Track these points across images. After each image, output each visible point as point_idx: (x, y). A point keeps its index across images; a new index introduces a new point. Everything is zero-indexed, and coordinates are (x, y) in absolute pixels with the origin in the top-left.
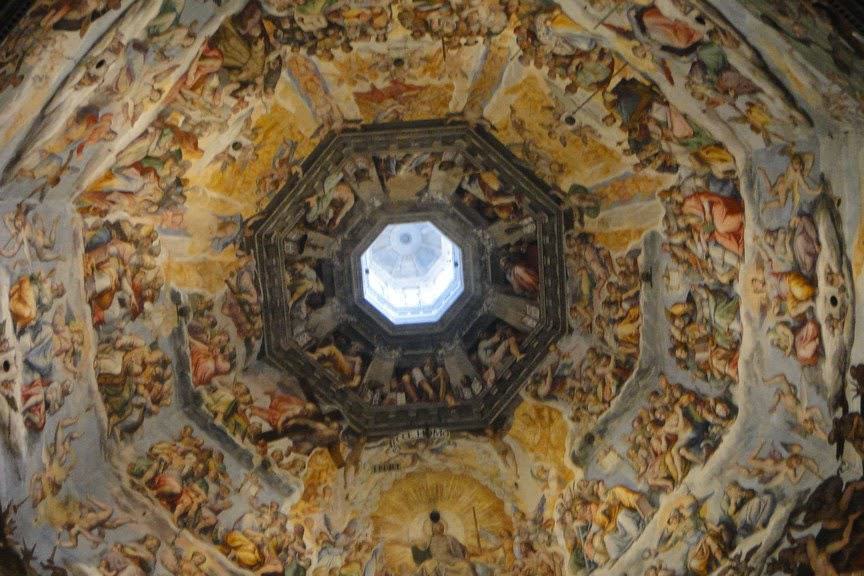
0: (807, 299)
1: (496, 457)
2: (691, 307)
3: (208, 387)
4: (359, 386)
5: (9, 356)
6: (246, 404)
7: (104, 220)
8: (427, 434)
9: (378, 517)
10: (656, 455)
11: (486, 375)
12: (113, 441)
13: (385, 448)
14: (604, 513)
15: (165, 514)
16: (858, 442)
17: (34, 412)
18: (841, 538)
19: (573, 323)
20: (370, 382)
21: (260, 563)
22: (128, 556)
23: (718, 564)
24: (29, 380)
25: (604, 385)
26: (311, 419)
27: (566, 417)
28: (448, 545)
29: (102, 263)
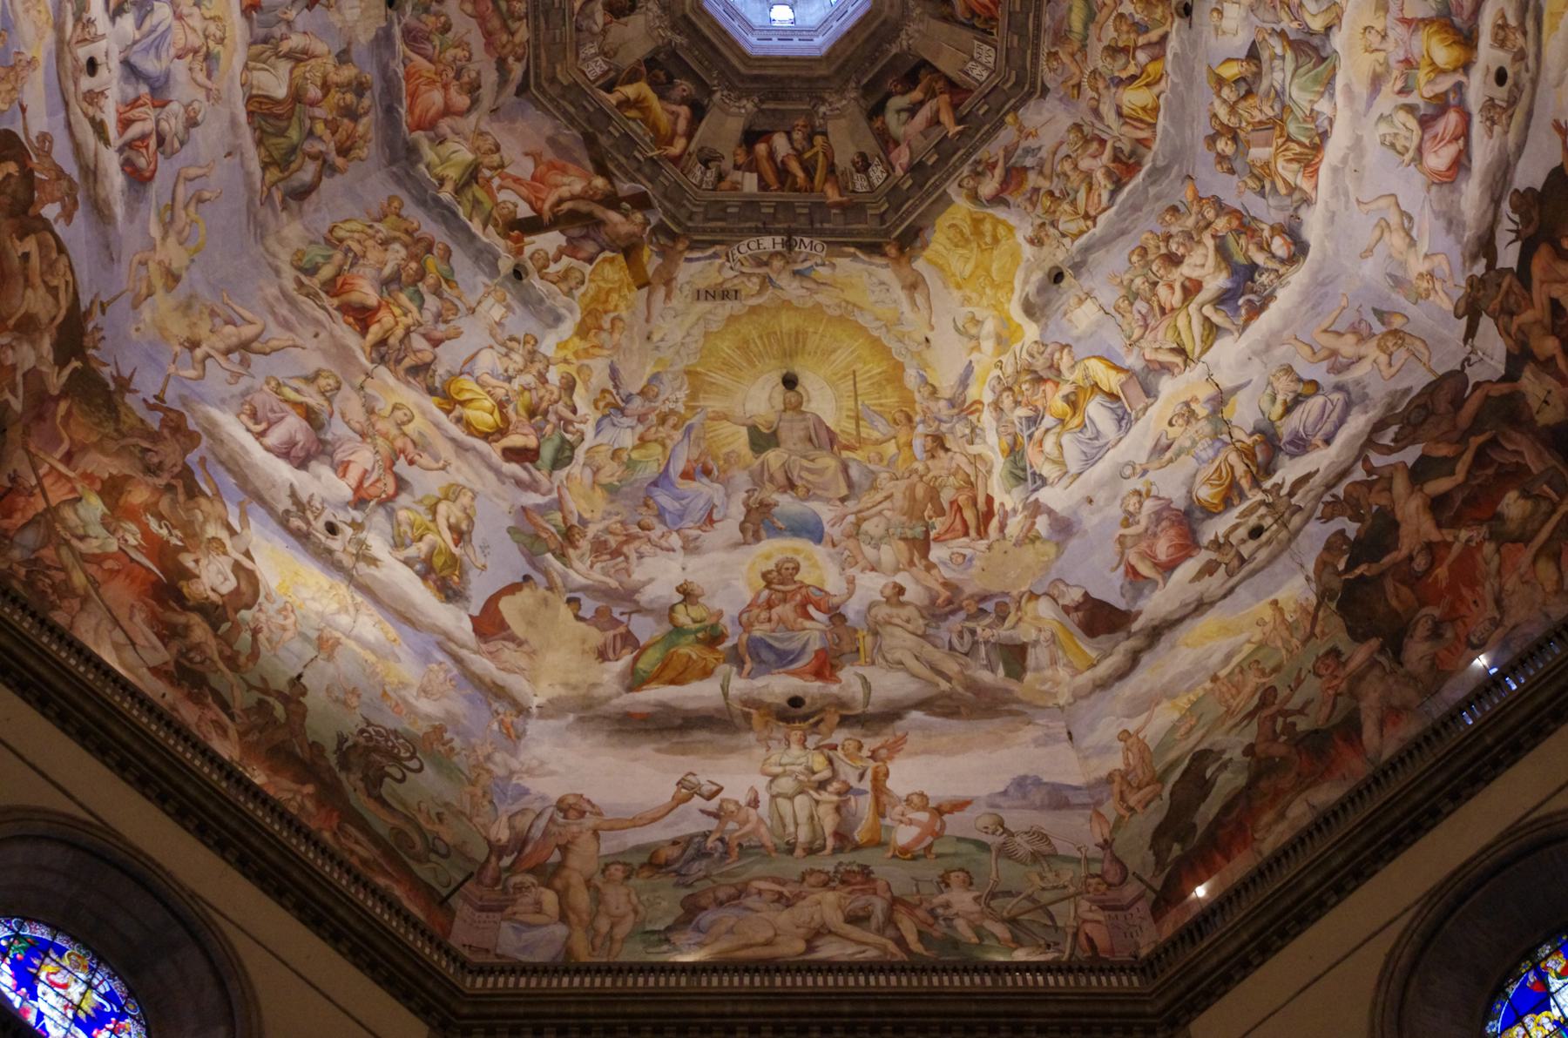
0: (1455, 70)
1: (900, 294)
2: (1254, 69)
3: (432, 134)
4: (680, 157)
5: (97, 50)
6: (495, 169)
8: (789, 245)
9: (697, 373)
10: (1163, 311)
11: (893, 155)
12: (269, 211)
13: (718, 262)
14: (1066, 398)
15: (351, 338)
16: (1504, 319)
18: (1452, 473)
19: (1048, 76)
20: (701, 150)
21: (502, 432)
22: (287, 401)
23: (1242, 496)
24: (131, 92)
25: (1090, 188)
26: (600, 202)
27: (1020, 237)
28: (807, 428)
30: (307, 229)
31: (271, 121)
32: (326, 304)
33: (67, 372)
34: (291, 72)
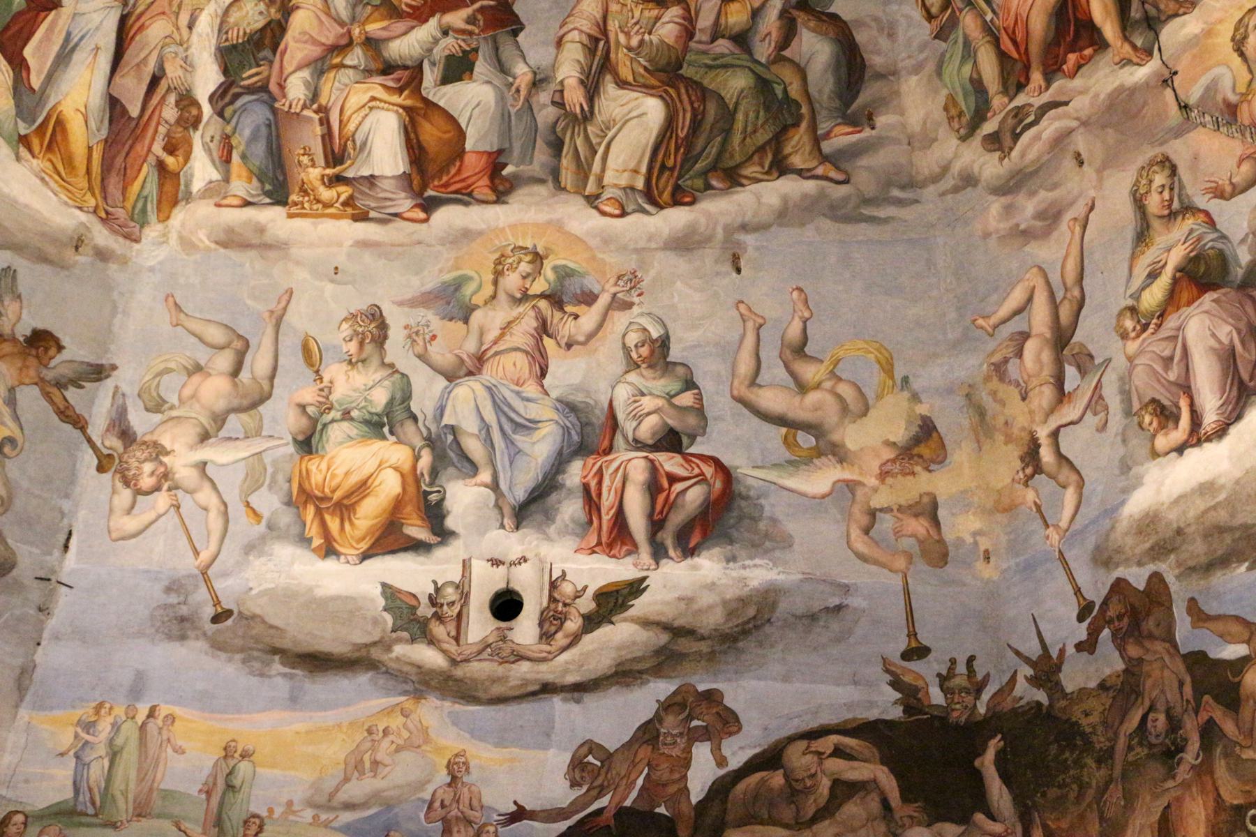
5: (486, 583)
7: (207, 109)
12: (864, 161)
17: (670, 506)
24: (571, 509)
29: (327, 137)
30: (917, 69)
31: (700, 143)
32: (1038, 101)
33: (998, 792)
34: (622, 84)
